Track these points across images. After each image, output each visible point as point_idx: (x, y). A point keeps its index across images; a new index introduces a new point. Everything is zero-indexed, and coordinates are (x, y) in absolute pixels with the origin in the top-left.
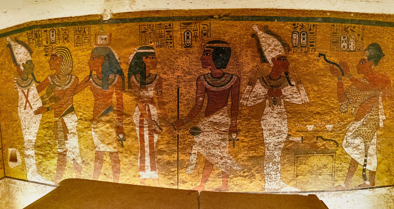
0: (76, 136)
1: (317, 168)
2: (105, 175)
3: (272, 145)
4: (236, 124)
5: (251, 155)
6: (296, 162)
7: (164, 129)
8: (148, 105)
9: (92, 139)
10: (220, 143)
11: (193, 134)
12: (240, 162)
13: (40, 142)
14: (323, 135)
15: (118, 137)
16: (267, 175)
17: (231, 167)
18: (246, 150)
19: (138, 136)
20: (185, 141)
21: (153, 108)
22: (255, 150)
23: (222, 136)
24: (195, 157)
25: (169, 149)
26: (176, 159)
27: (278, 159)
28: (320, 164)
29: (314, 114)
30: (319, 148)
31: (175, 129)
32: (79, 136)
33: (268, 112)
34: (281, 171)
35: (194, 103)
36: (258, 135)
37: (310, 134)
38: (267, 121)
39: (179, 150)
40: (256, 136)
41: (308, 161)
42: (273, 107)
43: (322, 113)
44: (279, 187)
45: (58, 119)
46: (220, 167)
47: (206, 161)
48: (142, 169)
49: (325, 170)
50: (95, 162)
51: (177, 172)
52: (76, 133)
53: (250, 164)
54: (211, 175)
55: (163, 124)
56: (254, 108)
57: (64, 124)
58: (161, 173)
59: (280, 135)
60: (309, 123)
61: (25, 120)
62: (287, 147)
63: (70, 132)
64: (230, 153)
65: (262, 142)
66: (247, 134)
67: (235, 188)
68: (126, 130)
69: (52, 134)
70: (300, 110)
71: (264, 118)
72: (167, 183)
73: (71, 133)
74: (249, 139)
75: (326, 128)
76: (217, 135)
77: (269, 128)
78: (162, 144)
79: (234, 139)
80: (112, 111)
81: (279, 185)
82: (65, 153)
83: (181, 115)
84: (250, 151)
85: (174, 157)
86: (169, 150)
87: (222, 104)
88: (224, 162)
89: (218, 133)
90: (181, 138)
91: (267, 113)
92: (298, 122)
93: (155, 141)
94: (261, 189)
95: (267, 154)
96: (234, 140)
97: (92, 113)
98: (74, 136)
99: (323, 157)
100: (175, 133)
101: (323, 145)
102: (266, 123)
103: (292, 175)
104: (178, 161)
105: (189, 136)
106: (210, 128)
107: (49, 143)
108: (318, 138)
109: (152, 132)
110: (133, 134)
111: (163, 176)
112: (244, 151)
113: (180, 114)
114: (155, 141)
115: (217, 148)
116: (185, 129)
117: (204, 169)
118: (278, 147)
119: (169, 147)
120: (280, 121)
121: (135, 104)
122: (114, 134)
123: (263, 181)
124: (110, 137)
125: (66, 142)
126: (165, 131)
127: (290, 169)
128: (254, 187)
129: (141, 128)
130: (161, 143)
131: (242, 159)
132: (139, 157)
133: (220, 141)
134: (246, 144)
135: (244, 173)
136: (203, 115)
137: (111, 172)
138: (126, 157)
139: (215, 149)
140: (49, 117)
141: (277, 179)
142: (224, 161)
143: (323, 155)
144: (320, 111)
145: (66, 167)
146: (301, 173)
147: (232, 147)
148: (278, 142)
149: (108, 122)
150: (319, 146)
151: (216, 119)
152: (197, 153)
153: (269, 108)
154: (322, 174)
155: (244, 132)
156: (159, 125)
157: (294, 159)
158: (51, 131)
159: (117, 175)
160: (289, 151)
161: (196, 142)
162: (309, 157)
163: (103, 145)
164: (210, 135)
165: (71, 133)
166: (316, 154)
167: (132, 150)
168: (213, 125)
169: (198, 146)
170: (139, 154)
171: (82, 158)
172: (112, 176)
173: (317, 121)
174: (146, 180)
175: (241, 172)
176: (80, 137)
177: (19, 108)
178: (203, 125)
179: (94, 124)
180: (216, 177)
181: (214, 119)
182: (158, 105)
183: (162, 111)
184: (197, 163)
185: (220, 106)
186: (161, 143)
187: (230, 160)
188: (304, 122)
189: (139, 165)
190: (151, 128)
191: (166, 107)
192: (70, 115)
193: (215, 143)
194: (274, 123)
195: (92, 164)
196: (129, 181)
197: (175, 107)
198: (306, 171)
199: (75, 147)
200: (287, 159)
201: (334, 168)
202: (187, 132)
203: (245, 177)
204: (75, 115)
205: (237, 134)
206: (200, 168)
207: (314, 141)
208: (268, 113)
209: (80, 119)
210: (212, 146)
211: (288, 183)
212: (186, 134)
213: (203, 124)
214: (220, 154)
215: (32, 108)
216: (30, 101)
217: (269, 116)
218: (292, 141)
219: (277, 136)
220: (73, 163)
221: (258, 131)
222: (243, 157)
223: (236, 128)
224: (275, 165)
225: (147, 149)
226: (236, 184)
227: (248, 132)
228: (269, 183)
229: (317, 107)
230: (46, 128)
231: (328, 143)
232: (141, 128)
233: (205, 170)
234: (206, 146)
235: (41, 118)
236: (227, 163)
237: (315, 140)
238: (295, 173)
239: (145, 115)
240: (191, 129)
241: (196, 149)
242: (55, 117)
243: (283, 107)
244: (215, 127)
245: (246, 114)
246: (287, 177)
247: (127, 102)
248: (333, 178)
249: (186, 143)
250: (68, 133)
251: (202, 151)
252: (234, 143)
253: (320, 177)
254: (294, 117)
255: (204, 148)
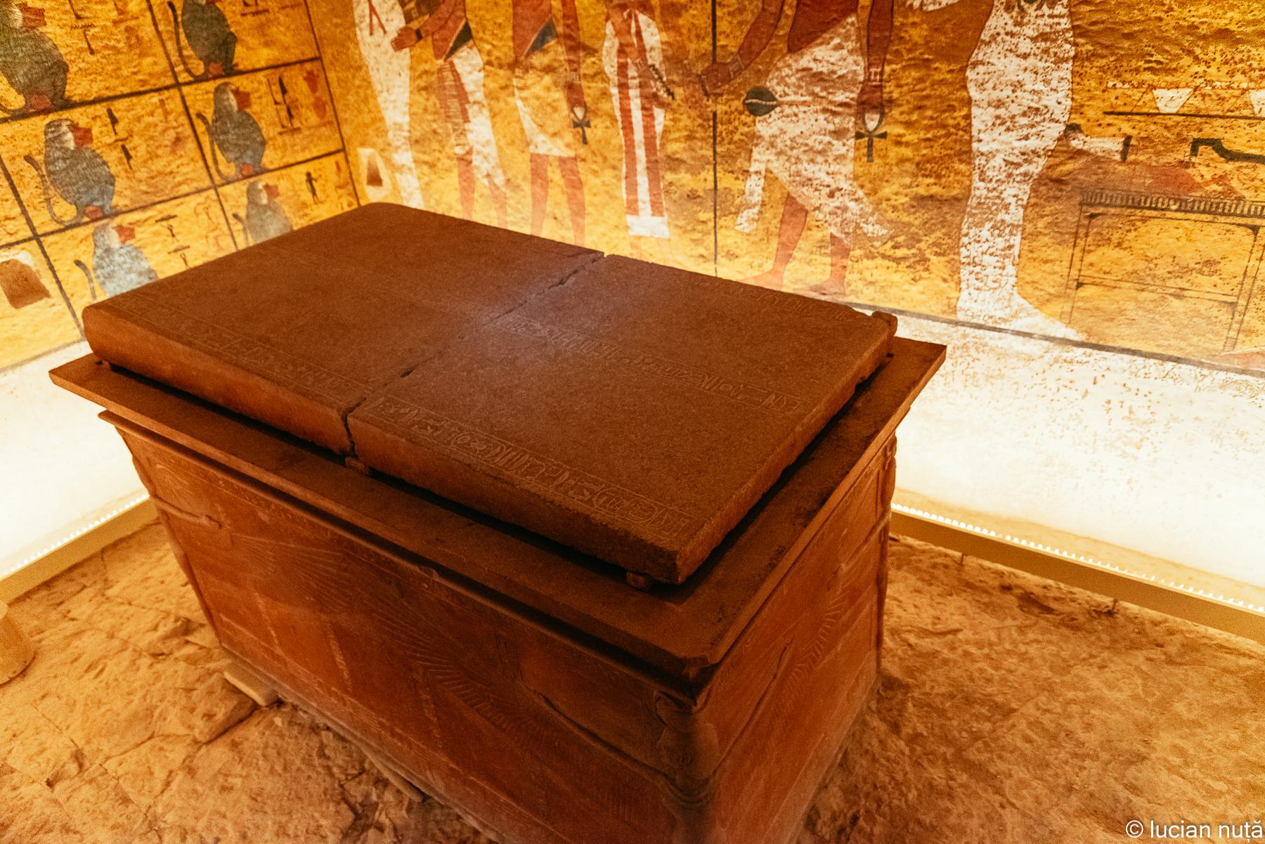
0: (486, 112)
1: (1171, 269)
2: (555, 218)
3: (998, 161)
4: (881, 80)
5: (922, 191)
6: (1082, 231)
7: (679, 92)
8: (636, 16)
9: (519, 121)
10: (829, 143)
11: (755, 111)
12: (886, 211)
13: (419, 128)
14: (1227, 136)
15: (572, 115)
16: (969, 264)
17: (858, 226)
18: (906, 171)
19: (618, 114)
20: (732, 132)
21: (649, 26)
22: (939, 177)
23: (837, 120)
24: (759, 183)
25: (694, 154)
26: (710, 185)
27: (1015, 215)
28: (1189, 255)
29: (1204, 37)
30: (1199, 186)
31: (707, 94)
32: (491, 110)
33: (998, 34)
34: (1019, 256)
35: (757, 6)
36: (951, 122)
37: (1166, 127)
38: (992, 69)
39: (718, 160)
40: (944, 126)
41: (1133, 234)
42: (1022, 9)
43: (1246, 34)
44: (1008, 311)
45: (441, 62)
46: (826, 222)
47: (789, 200)
48: (632, 207)
49: (1205, 281)
50: (533, 182)
51: (712, 224)
52: (485, 102)
53: (917, 222)
54: (800, 242)
55: (675, 78)
56: (946, 16)
57: (457, 77)
58: (675, 222)
59: (1032, 126)
60: (1169, 79)
61: (377, 66)
62: (1055, 174)
63: (471, 99)
64: (856, 178)
65: (965, 149)
66: (914, 117)
67: (866, 292)
68: (589, 95)
69: (438, 105)
70: (1138, 21)
71: (980, 57)
72: (689, 253)
73: (475, 103)
74: (922, 135)
75: (1247, 105)
76: (821, 117)
77: (996, 95)
78: (677, 140)
79: (870, 133)
80: (553, 38)
81: (1006, 303)
82: (468, 157)
83: (723, 47)
84: (920, 179)
85: (705, 180)
86: (694, 158)
87: (840, 7)
88: (838, 208)
89: (825, 110)
90: (722, 124)
91: (993, 38)
92: (1118, 76)
93: (659, 129)
94: (946, 308)
95: (978, 193)
96: (870, 134)
97: (511, 44)
98: (480, 111)
99: (1210, 229)
100: (707, 107)
101: (1220, 179)
102: (987, 77)
103: (1059, 279)
104: (715, 193)
105: (743, 117)
106: (800, 92)
107: (435, 132)
108: (1201, 148)
109: (651, 100)
110: (605, 106)
111: (680, 231)
112: (901, 175)
113: (719, 44)
114: (659, 129)
115: (820, 159)
116: (733, 93)
117: (782, 222)
118: (1022, 170)
119: (693, 150)
120: (1041, 71)
121: (603, 13)
122: (564, 106)
123: (953, 284)
124: (556, 116)
125: (467, 126)
126: (682, 100)
127: (1054, 255)
128: (923, 297)
129: (623, 87)
130: (673, 136)
131: (895, 203)
132: (624, 174)
133: (827, 139)
134: (908, 152)
135: (895, 247)
136: (782, 46)
137: (567, 212)
138: (595, 173)
139: (812, 161)
140: (424, 57)
141: (1003, 283)
142: (837, 204)
143: (1210, 217)
144: (1233, 27)
145: (476, 195)
146: (1096, 275)
147: (865, 159)
148: (1023, 150)
149: (548, 69)
150: (1198, 179)
151: (820, 62)
152: (763, 173)
153: (1006, 16)
154: (1186, 293)
155: (905, 108)
156: (665, 79)
157: (1079, 221)
158: (433, 99)
159: (580, 220)
160: (1061, 190)
161: (760, 137)
162: (1144, 220)
163: (541, 138)
164: (801, 115)
165: (475, 103)
166: (1177, 211)
167: (609, 156)
168: (811, 83)
169: (768, 149)
170: (624, 166)
171: (505, 172)
172: (570, 223)
173: (1213, 70)
174: (642, 241)
175: (886, 243)
176: (494, 115)
177: (358, 32)
178: (782, 80)
179: (517, 77)
180: (814, 249)
181: (815, 60)
182: (662, 13)
183: (672, 34)
184: (763, 204)
185: (835, 16)
186: (673, 136)
187: (856, 200)
188: (1147, 76)
189: (625, 196)
190: (647, 91)
191: (681, 22)
192: (464, 52)
193: (816, 141)
194: (1017, 79)
195: (527, 187)
196: (606, 239)
197: (704, 22)
198: (1117, 273)
199: (488, 142)
200: (1049, 219)
201: (1248, 281)
202: (737, 104)
203: (898, 260)
204: (475, 49)
205: (883, 114)
206: (773, 217)
207: (1180, 157)
208: (999, 39)
209: (489, 63)
210: (805, 151)
211: (1042, 304)
212: (736, 110)
213: (782, 78)
214: (828, 180)
215: (385, 32)
216: (378, 10)
217: (1000, 48)
218: (1080, 153)
219: (1022, 127)
220: (487, 184)
221: (952, 108)
222: (896, 194)
223: (879, 94)
224: (999, 236)
225: (640, 153)
226: (869, 279)
227: (920, 108)
228: (975, 293)
229: (1222, 7)
230: (425, 89)
231: (1245, 171)
232: (623, 87)
233: (785, 227)
234: (789, 152)
235: (407, 61)
236: (845, 209)
237: (1183, 152)
238: (1074, 273)
239: (630, 48)
240: (748, 93)
241: (761, 158)
242: (437, 57)
243: (1065, 11)
244: (817, 90)
245: (916, 44)
246: (1042, 281)
247: (585, 9)
248: (1237, 318)
249: (737, 137)
250: (469, 102)
251: (778, 167)
252: (870, 146)
253: (1176, 303)
254: (1105, 52)
255: (783, 158)
